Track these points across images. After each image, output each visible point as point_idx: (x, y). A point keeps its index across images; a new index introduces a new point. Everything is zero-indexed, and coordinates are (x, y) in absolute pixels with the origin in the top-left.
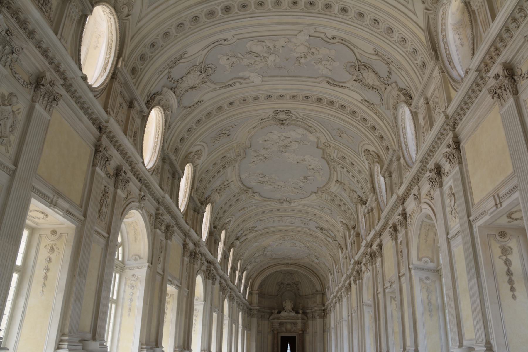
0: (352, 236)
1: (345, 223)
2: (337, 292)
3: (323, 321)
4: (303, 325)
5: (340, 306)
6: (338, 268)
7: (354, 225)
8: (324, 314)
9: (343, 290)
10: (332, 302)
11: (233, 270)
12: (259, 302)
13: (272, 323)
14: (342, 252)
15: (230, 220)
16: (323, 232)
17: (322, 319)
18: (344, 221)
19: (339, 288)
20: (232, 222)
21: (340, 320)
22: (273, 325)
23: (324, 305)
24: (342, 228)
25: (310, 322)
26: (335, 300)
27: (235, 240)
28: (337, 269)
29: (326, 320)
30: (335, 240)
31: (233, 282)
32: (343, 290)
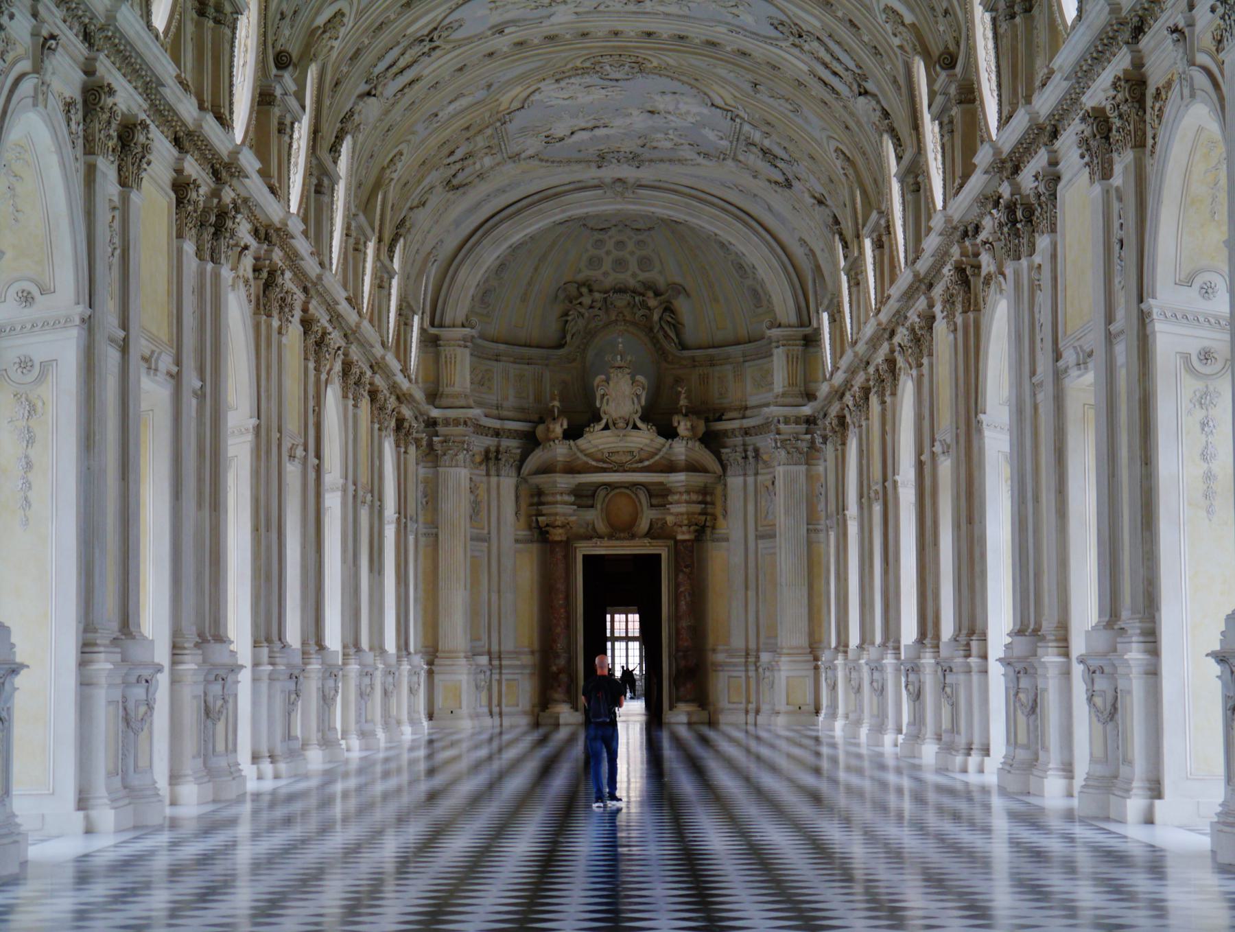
0: (939, 99)
1: (913, 25)
2: (874, 343)
3: (810, 477)
4: (700, 498)
5: (884, 411)
6: (877, 223)
7: (952, 47)
8: (812, 444)
9: (902, 336)
10: (847, 385)
11: (352, 241)
12: (481, 381)
13: (539, 493)
14: (899, 158)
15: (340, 14)
16: (806, 47)
17: (803, 468)
18: (909, 18)
19: (879, 324)
20: (345, 20)
21: (885, 480)
22: (550, 499)
23: (810, 396)
24: (896, 41)
25: (734, 482)
26: (859, 380)
27: (361, 96)
28: (873, 231)
29: (821, 469)
30: (865, 93)
31: (354, 301)
32: (902, 336)
